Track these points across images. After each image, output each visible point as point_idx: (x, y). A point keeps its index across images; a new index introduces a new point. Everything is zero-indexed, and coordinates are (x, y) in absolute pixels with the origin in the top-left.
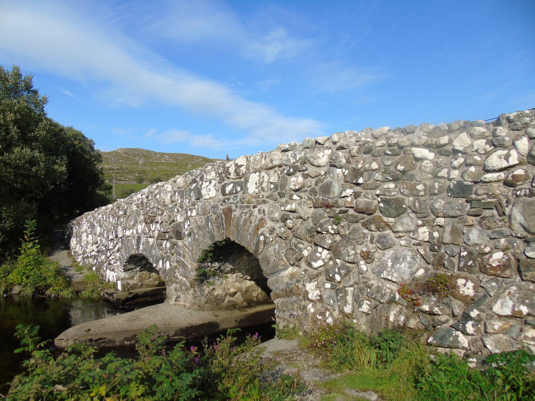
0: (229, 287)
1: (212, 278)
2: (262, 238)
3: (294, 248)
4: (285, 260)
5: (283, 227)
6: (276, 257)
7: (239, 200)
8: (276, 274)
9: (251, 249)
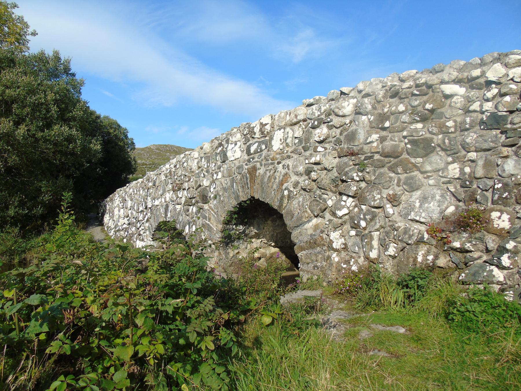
1: (237, 242)
2: (286, 193)
3: (318, 199)
4: (309, 212)
5: (307, 180)
6: (299, 210)
7: (264, 158)
8: (300, 227)
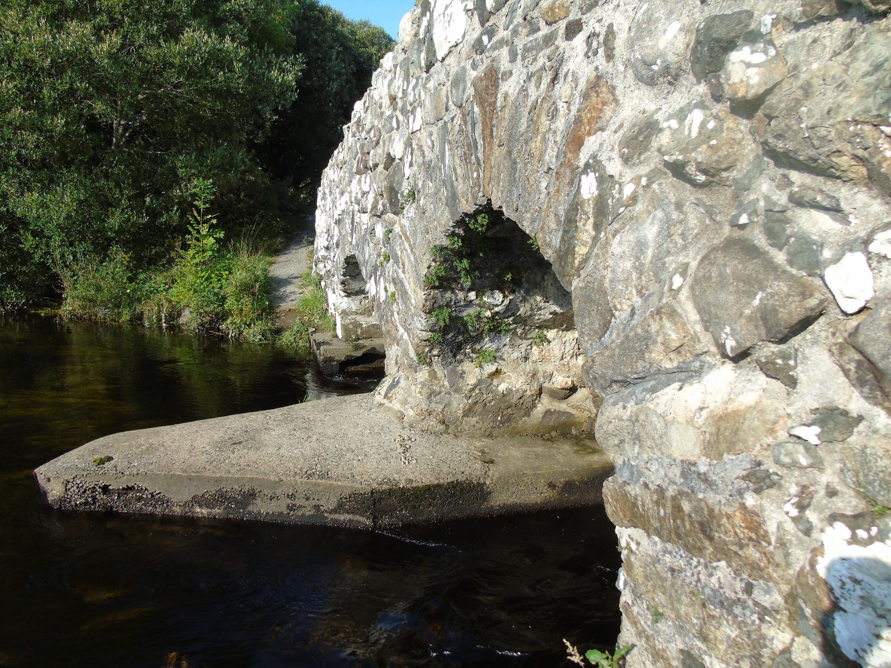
0: (549, 368)
1: (492, 341)
2: (589, 186)
3: (760, 239)
4: (692, 315)
5: (701, 105)
6: (640, 293)
7: (520, 20)
8: (638, 389)
9: (549, 245)
